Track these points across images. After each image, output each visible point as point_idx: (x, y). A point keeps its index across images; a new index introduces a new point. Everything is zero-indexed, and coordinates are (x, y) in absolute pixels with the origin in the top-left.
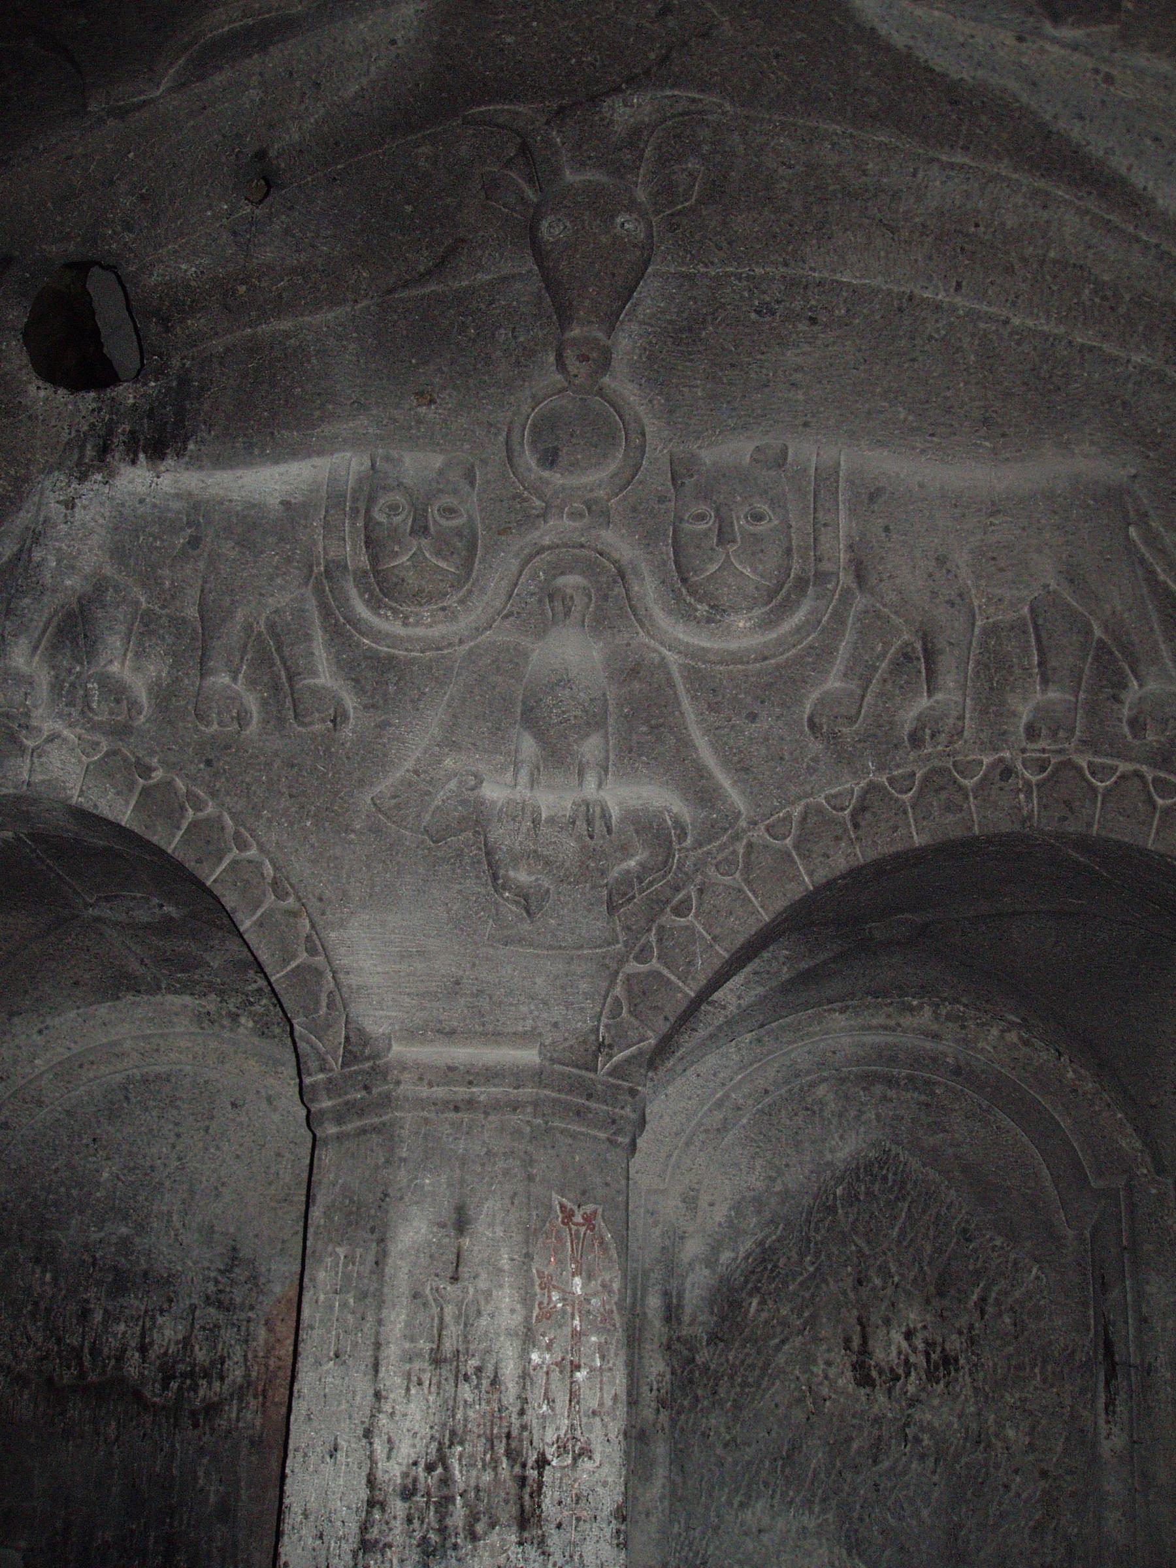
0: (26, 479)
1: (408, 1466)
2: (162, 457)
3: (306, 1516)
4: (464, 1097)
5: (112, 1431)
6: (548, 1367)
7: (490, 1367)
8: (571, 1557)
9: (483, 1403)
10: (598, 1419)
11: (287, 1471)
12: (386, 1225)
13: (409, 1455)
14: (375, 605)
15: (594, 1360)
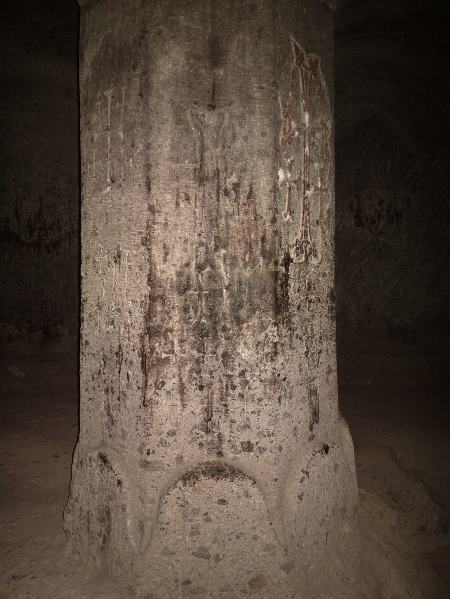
1: (181, 267)
3: (100, 308)
6: (290, 185)
7: (246, 183)
8: (306, 329)
9: (241, 214)
10: (319, 227)
11: (82, 274)
12: (147, 58)
13: (182, 258)
15: (317, 182)
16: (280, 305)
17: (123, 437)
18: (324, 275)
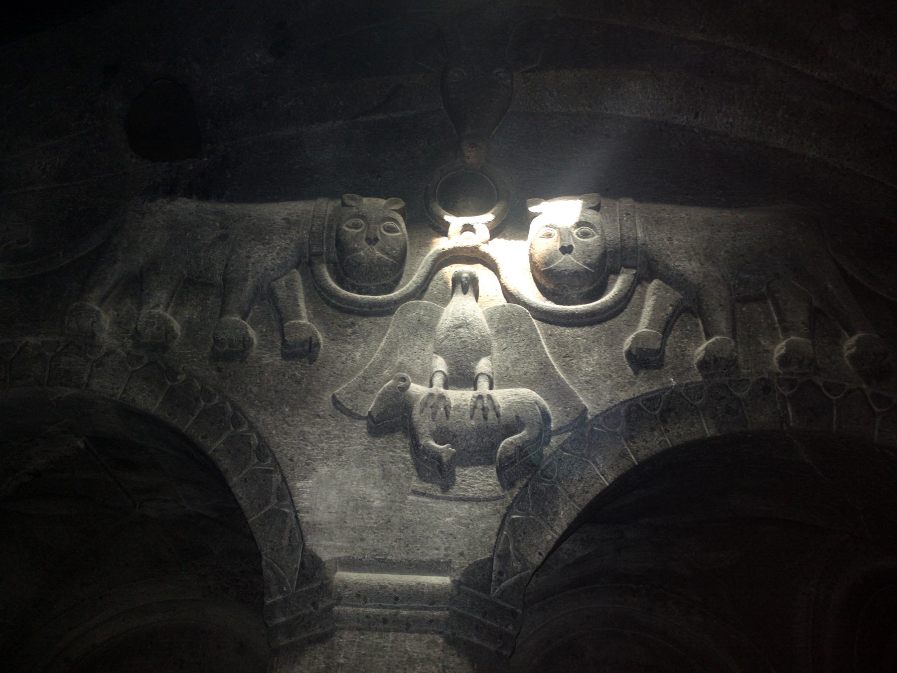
14: (341, 282)
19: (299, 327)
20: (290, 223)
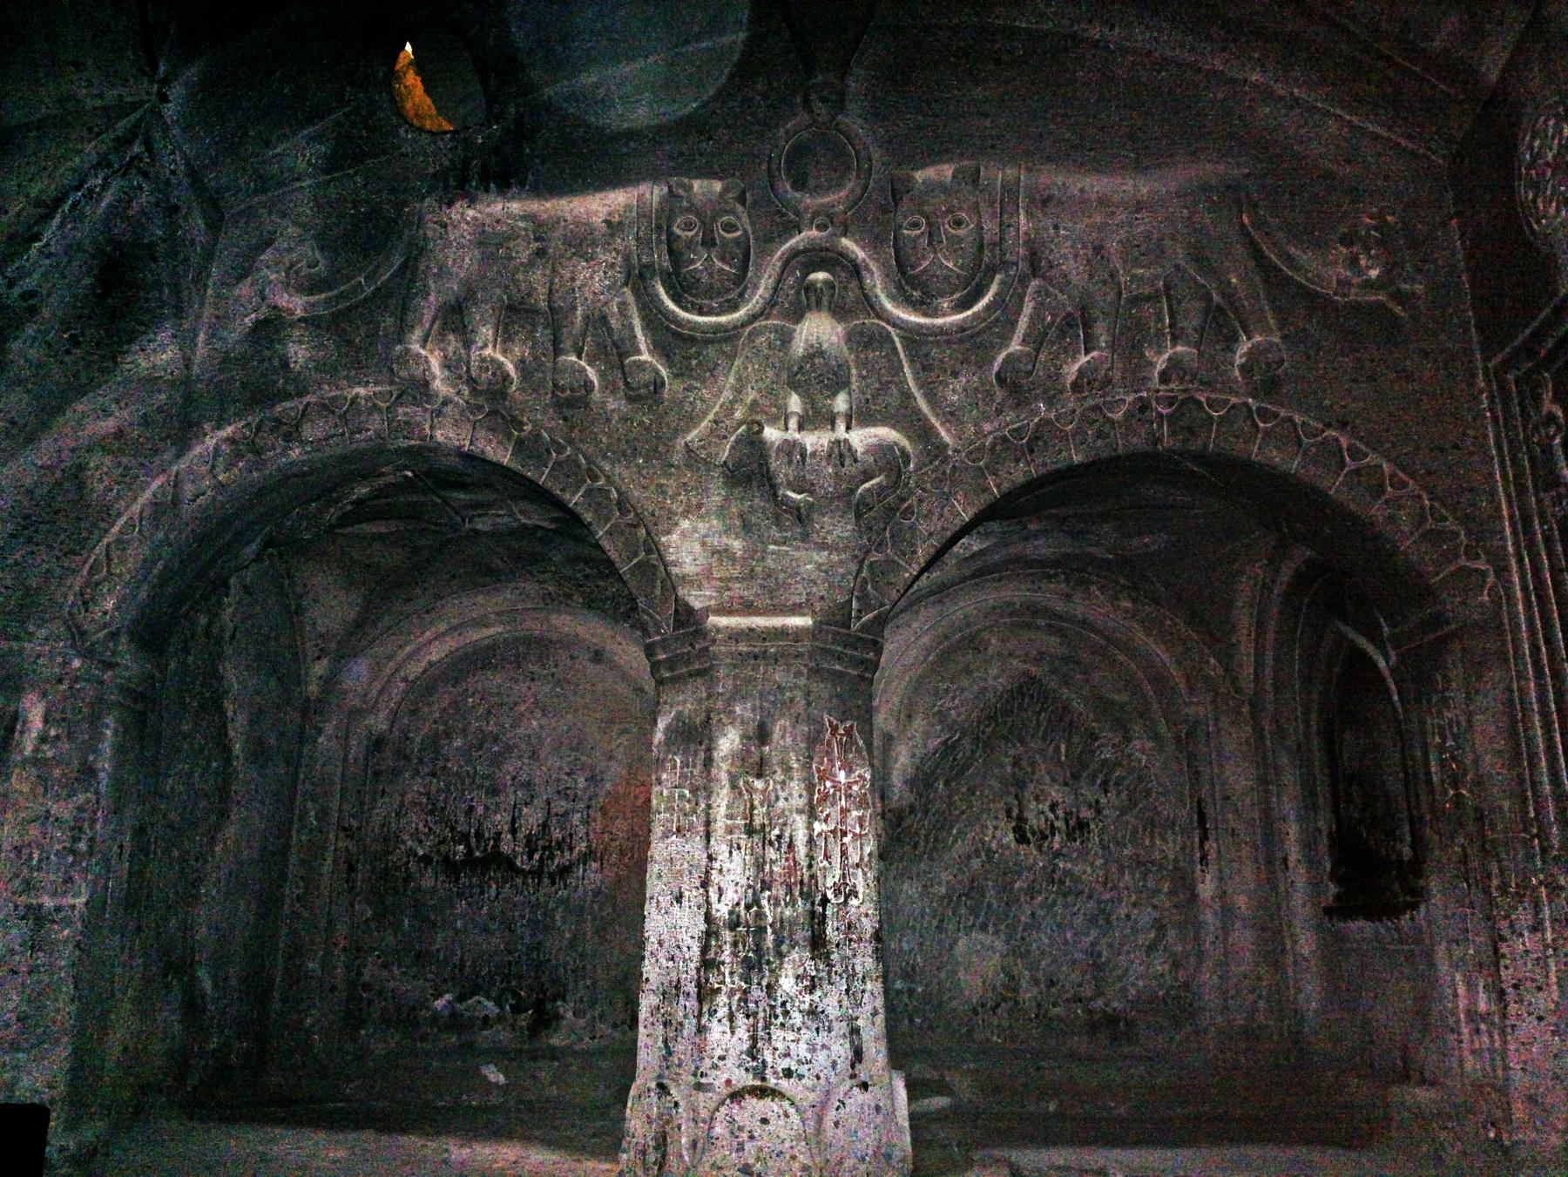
0: (405, 204)
2: (509, 186)
4: (762, 650)
5: (493, 892)
7: (787, 835)
12: (711, 739)
14: (677, 299)
16: (818, 943)
17: (679, 1066)
18: (867, 915)
19: (640, 366)
20: (614, 227)
